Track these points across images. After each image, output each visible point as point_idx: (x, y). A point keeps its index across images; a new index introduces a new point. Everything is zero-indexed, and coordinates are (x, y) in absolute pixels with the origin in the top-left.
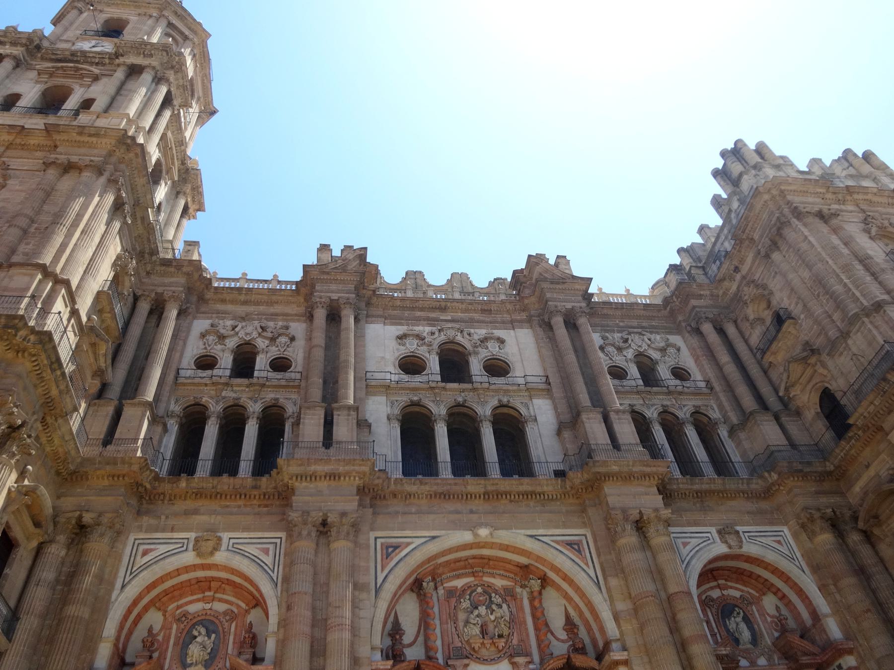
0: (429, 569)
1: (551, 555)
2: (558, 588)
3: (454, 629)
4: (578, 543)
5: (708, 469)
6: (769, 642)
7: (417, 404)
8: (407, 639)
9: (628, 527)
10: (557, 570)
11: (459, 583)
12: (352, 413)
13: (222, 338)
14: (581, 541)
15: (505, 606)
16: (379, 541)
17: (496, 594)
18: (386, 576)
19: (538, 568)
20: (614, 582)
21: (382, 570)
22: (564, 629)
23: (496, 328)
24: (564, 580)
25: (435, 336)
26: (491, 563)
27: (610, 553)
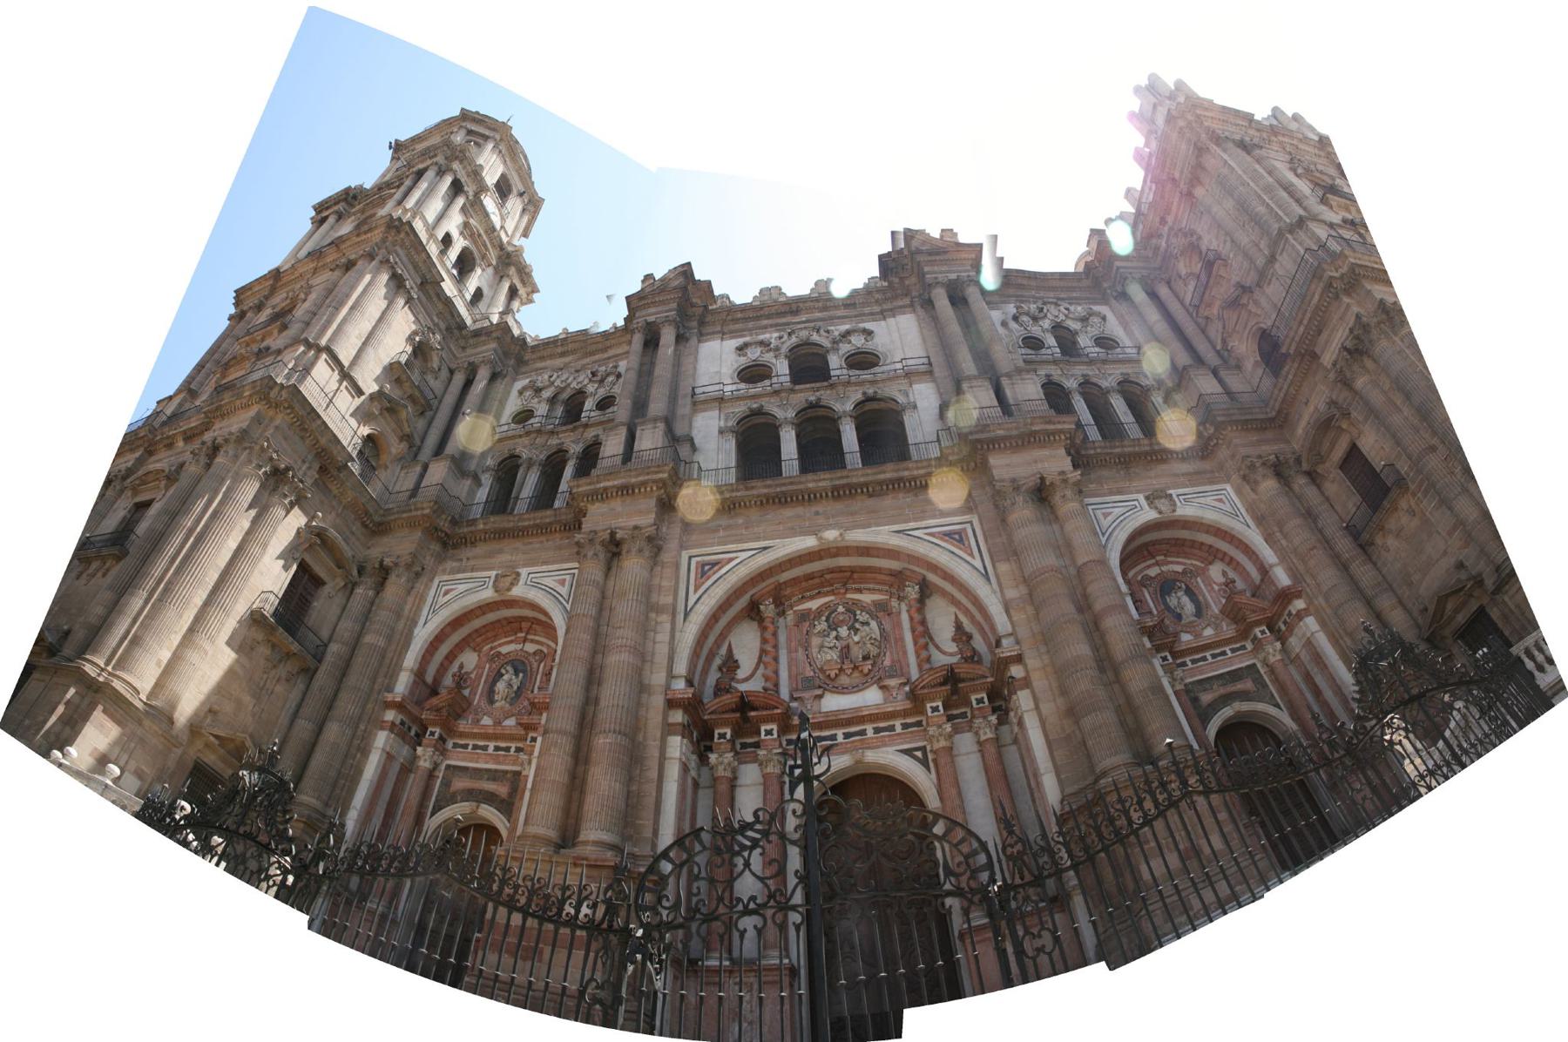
0: (767, 589)
1: (922, 549)
2: (944, 594)
4: (959, 533)
6: (1217, 611)
7: (759, 412)
8: (741, 674)
9: (1020, 499)
10: (934, 567)
11: (814, 605)
12: (659, 424)
13: (538, 391)
14: (965, 529)
15: (874, 624)
16: (694, 561)
17: (862, 611)
18: (700, 597)
19: (914, 572)
20: (1003, 567)
21: (696, 591)
22: (954, 640)
24: (944, 579)
25: (782, 340)
26: (855, 576)
27: (1000, 535)
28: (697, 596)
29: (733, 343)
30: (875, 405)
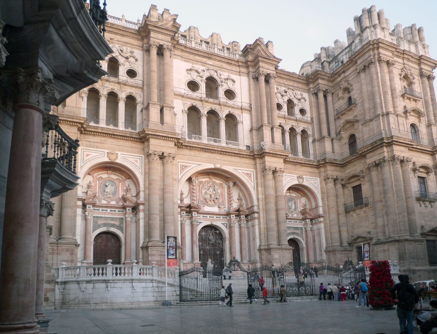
3: (201, 195)
5: (300, 155)
8: (184, 196)
11: (204, 180)
23: (232, 73)
28: (182, 174)
29: (189, 65)
30: (230, 115)
